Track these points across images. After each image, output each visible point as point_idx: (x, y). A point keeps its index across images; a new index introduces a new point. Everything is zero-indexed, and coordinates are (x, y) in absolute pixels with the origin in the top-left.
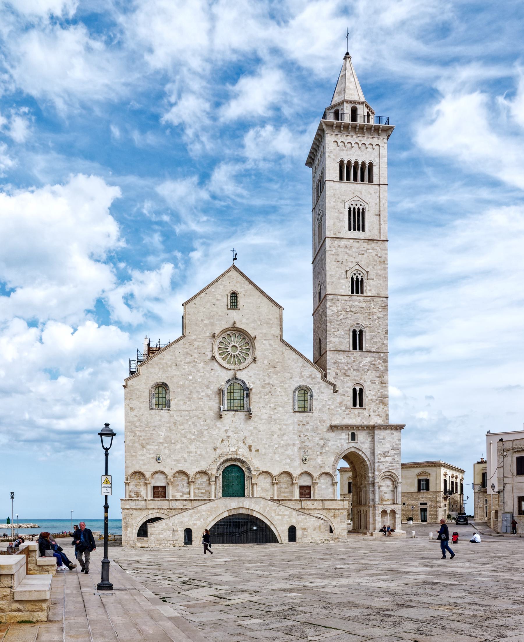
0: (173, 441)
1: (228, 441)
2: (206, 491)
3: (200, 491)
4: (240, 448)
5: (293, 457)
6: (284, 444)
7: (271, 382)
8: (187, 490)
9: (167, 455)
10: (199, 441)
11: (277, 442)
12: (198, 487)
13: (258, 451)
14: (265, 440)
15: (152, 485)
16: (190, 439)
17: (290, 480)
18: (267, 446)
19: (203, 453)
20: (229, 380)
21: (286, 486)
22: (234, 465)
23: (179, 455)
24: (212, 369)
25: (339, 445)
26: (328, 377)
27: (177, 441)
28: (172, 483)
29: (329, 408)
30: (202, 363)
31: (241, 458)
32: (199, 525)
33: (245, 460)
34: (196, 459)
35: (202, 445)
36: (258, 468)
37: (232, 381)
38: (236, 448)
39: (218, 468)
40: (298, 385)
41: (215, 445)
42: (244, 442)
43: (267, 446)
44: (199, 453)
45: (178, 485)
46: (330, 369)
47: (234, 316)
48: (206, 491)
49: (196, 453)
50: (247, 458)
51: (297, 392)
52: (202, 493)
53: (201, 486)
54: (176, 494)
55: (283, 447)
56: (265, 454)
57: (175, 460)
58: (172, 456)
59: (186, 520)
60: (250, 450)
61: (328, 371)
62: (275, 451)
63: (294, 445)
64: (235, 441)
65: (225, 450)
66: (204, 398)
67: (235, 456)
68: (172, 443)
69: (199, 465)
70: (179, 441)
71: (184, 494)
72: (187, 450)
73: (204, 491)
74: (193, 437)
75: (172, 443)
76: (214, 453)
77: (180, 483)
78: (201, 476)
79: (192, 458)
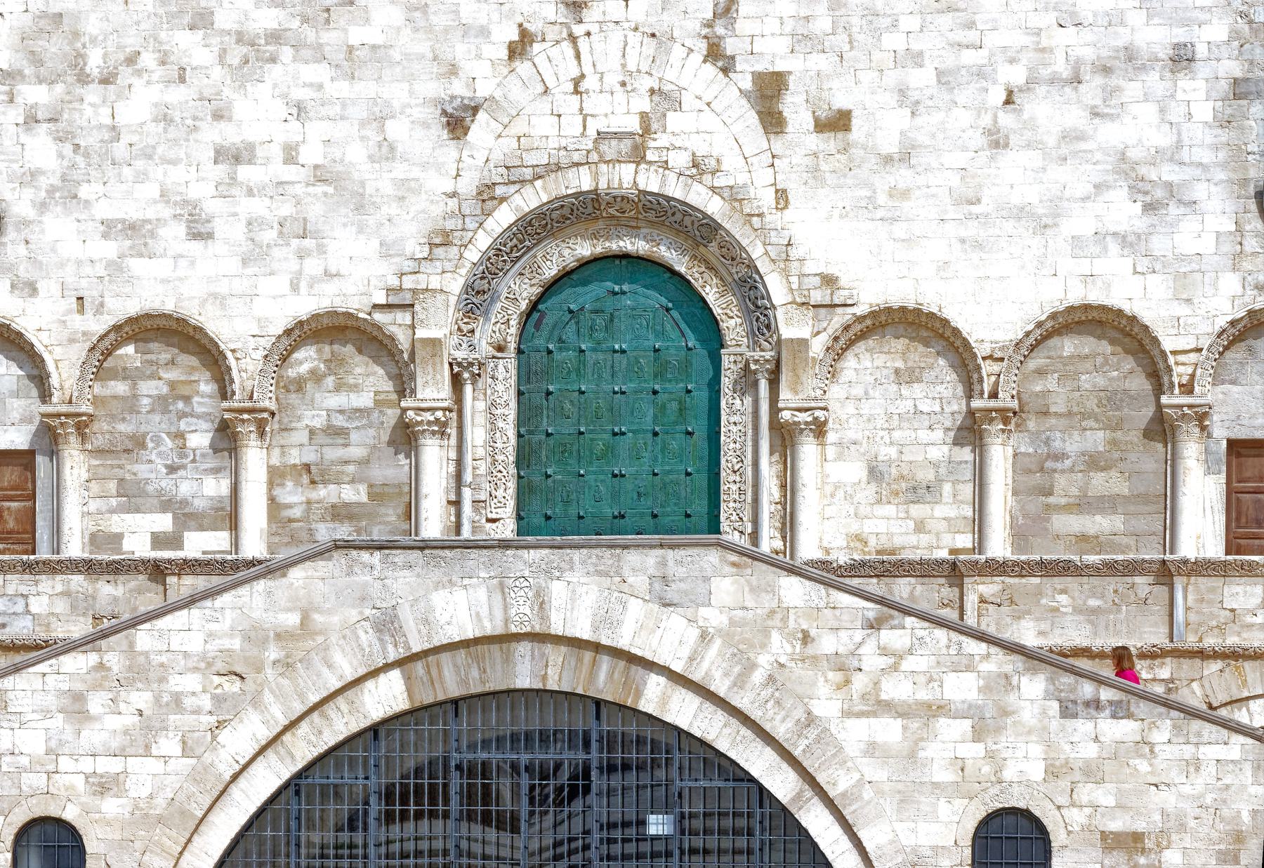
0: (94, 61)
1: (567, 47)
2: (378, 494)
3: (327, 493)
4: (678, 105)
5: (1169, 173)
6: (1088, 54)
8: (217, 487)
9: (44, 182)
10: (320, 56)
11: (1028, 40)
12: (310, 456)
13: (837, 123)
14: (908, 23)
16: (240, 38)
17: (1140, 383)
18: (921, 79)
19: (356, 154)
21: (1096, 439)
22: (625, 256)
23: (141, 178)
27: (131, 60)
28: (82, 426)
31: (675, 190)
32: (139, 788)
33: (714, 207)
34: (286, 209)
35: (342, 89)
36: (829, 281)
38: (644, 104)
39: (469, 288)
41: (458, 88)
42: (715, 53)
43: (921, 79)
44: (311, 154)
45: (138, 443)
48: (378, 494)
49: (290, 155)
50: (734, 196)
52: (339, 513)
53: (333, 454)
54: (117, 523)
55: (1077, 80)
56: (905, 157)
57: (109, 228)
58: (84, 192)
59: (32, 742)
60: (772, 121)
62: (1007, 120)
63: (1182, 59)
64: (634, 39)
65: (543, 126)
67: (624, 177)
68: (83, 79)
69: (313, 266)
70: (148, 60)
71: (187, 517)
72: (213, 134)
73: (353, 494)
75: (83, 79)
76: (450, 152)
77: (156, 424)
78: (335, 364)
79: (258, 207)
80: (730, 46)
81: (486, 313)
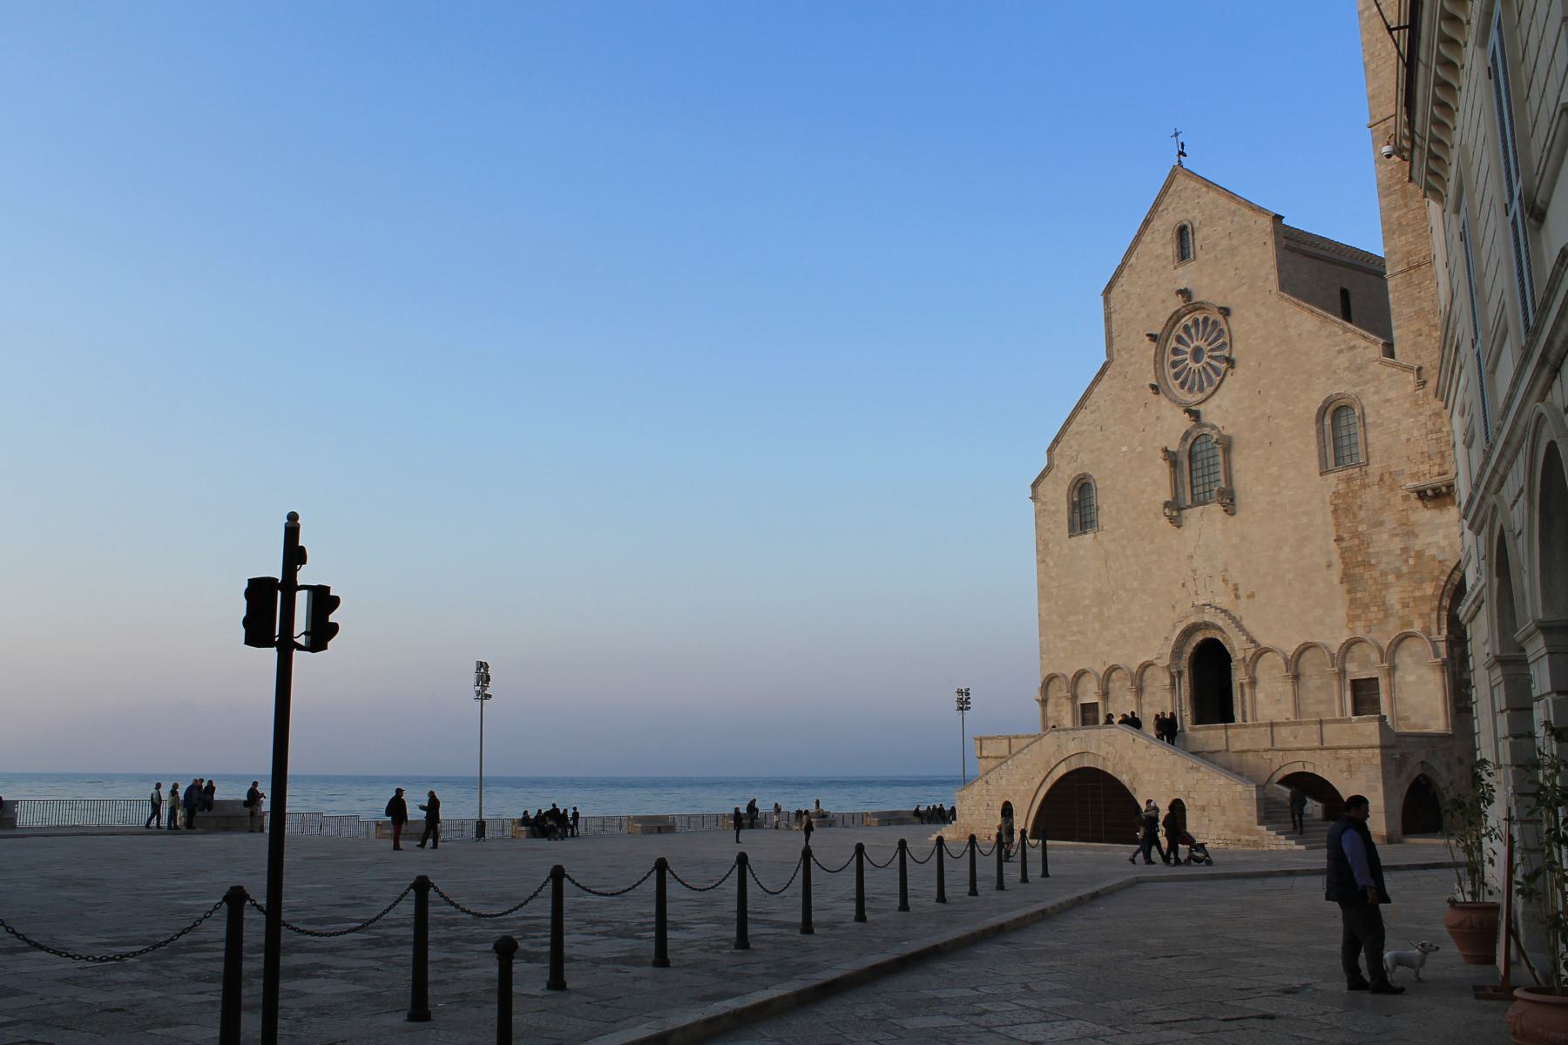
7: (1268, 411)
15: (1079, 703)
20: (1187, 434)
24: (1158, 418)
25: (1444, 543)
26: (1397, 350)
29: (1408, 440)
30: (1142, 410)
37: (1195, 435)
40: (1324, 398)
42: (1224, 580)
46: (1399, 327)
47: (1186, 276)
51: (1328, 421)
60: (1237, 597)
61: (1395, 334)
66: (1149, 489)
74: (1135, 584)
80: (1228, 578)
81: (1180, 658)
